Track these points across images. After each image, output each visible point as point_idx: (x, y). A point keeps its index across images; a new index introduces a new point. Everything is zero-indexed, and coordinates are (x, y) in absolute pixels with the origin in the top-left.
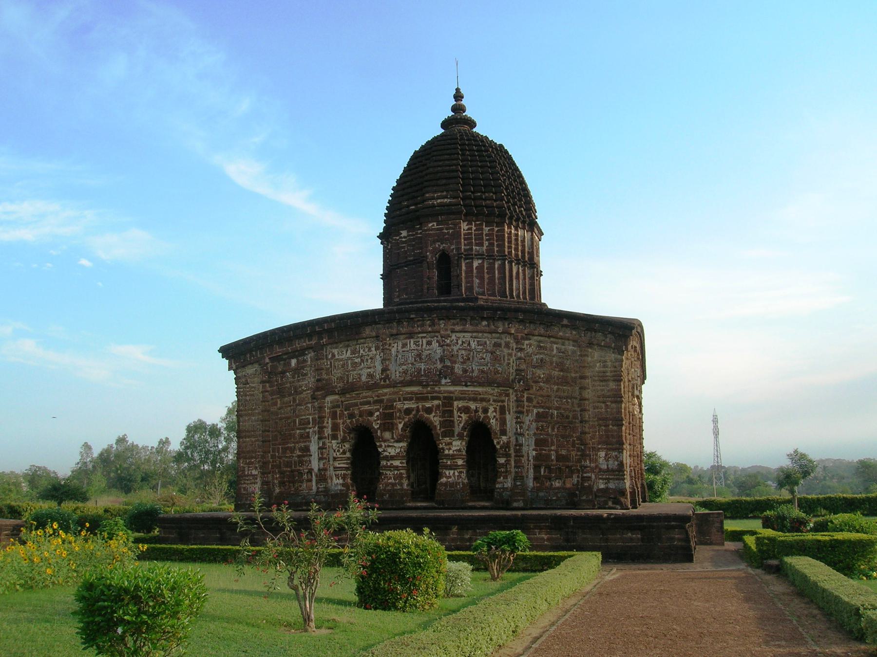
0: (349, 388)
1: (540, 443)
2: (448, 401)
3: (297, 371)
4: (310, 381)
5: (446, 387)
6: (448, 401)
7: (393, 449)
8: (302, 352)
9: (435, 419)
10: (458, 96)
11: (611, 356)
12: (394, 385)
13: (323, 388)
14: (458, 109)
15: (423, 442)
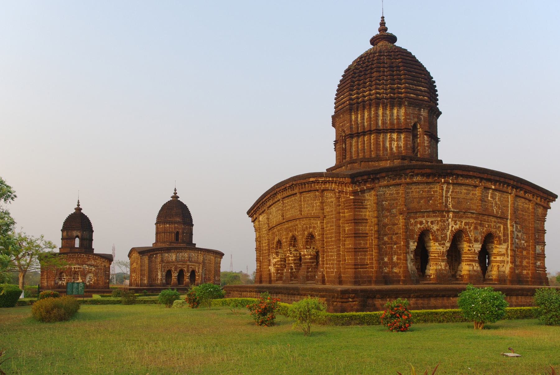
0: (168, 262)
1: (205, 275)
2: (188, 266)
3: (155, 258)
4: (159, 260)
5: (188, 263)
6: (188, 266)
7: (175, 275)
8: (157, 254)
9: (186, 269)
10: (175, 190)
11: (219, 259)
12: (178, 262)
13: (162, 261)
14: (175, 193)
15: (181, 274)
